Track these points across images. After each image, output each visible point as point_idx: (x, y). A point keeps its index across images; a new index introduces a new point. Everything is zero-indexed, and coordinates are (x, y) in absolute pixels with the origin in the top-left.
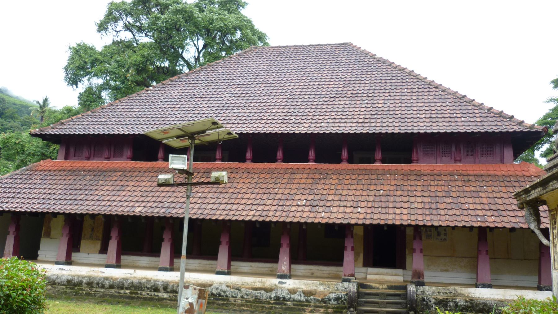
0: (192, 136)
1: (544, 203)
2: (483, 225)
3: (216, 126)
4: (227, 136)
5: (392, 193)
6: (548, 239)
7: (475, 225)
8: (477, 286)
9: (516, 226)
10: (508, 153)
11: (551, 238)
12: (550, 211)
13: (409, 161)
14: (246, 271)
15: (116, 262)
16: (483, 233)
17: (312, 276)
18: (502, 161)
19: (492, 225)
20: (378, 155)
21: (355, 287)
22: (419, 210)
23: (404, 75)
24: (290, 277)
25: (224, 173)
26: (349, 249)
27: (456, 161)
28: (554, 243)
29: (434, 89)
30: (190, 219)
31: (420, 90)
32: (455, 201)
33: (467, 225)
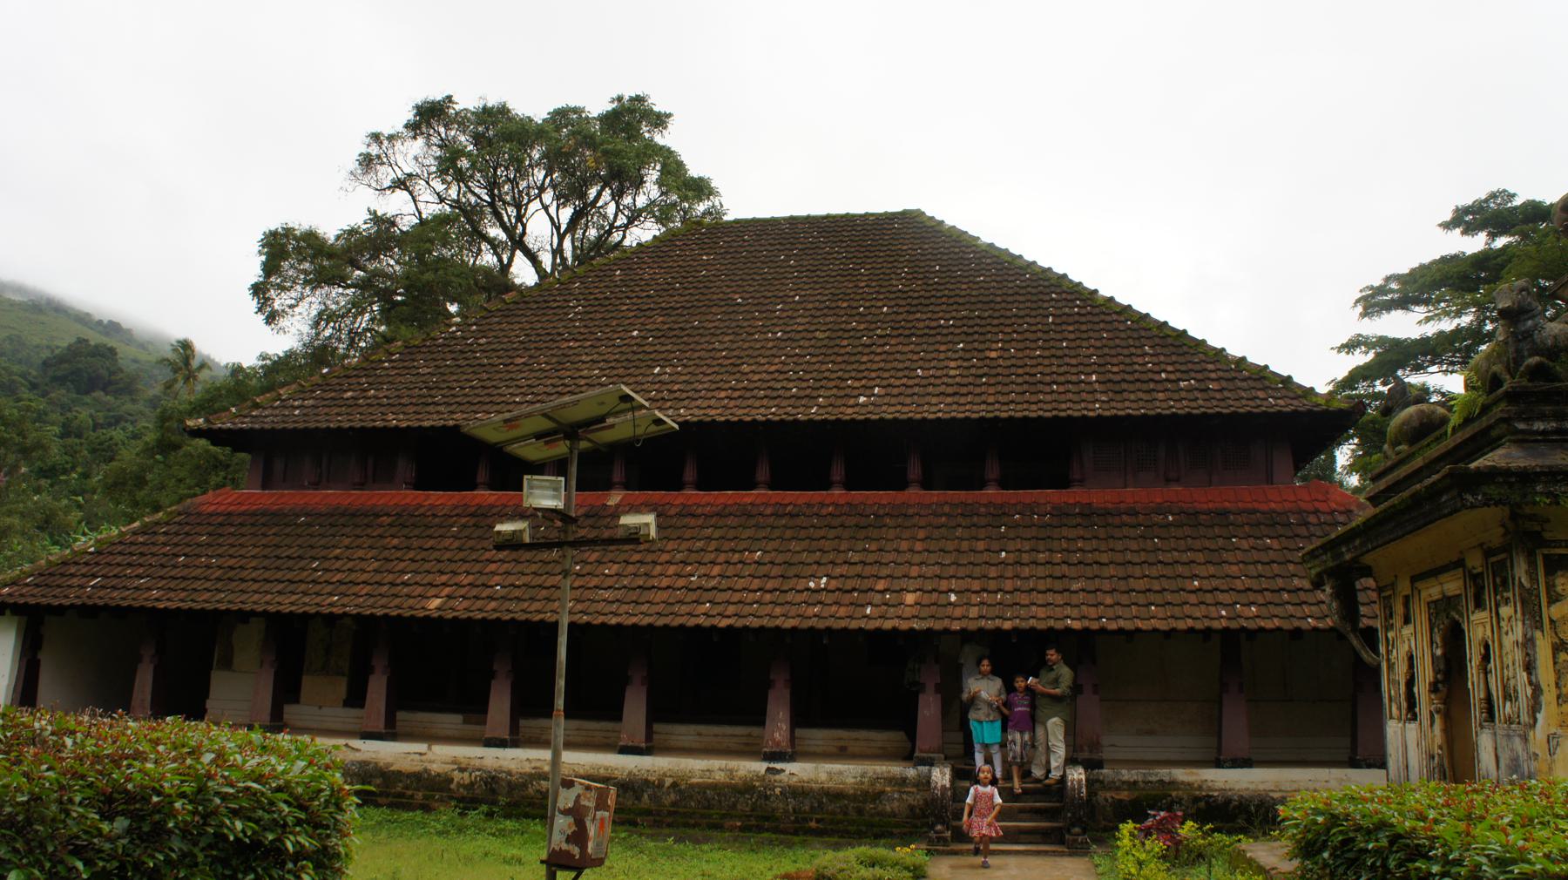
0: (571, 431)
1: (1367, 571)
2: (1234, 625)
3: (628, 405)
4: (653, 428)
5: (1026, 558)
6: (1376, 651)
7: (1216, 625)
8: (1218, 764)
9: (1303, 625)
10: (1283, 461)
11: (1382, 650)
12: (1380, 590)
13: (1063, 483)
14: (686, 745)
15: (386, 726)
16: (1232, 642)
17: (842, 754)
18: (1269, 480)
19: (1251, 625)
20: (993, 471)
21: (948, 777)
24: (791, 758)
25: (650, 519)
26: (930, 688)
27: (1168, 481)
28: (1388, 660)
30: (572, 625)
31: (1083, 319)
32: (1168, 571)
33: (1199, 625)
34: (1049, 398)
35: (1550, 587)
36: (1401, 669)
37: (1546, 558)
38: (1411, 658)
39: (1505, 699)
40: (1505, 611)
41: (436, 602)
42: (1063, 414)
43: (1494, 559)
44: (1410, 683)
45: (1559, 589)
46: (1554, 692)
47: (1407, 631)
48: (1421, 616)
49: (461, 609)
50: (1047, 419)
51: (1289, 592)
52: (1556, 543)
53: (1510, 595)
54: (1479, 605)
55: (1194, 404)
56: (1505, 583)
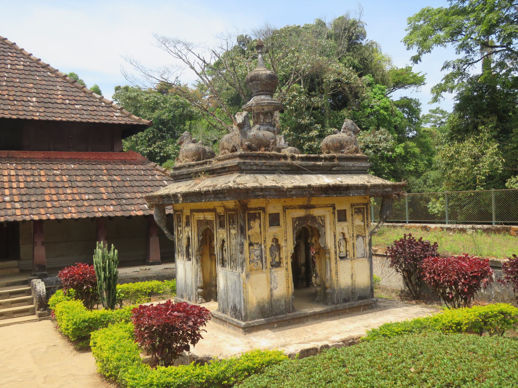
2: (105, 215)
6: (173, 234)
11: (175, 233)
22: (40, 203)
23: (5, 46)
29: (42, 69)
34: (13, 108)
35: (249, 223)
36: (184, 242)
37: (249, 214)
38: (188, 238)
39: (231, 260)
40: (233, 232)
42: (22, 117)
43: (230, 213)
44: (188, 247)
45: (251, 225)
46: (249, 260)
47: (187, 229)
48: (194, 224)
50: (14, 119)
51: (125, 199)
52: (252, 209)
53: (234, 226)
54: (222, 226)
55: (82, 117)
56: (233, 222)
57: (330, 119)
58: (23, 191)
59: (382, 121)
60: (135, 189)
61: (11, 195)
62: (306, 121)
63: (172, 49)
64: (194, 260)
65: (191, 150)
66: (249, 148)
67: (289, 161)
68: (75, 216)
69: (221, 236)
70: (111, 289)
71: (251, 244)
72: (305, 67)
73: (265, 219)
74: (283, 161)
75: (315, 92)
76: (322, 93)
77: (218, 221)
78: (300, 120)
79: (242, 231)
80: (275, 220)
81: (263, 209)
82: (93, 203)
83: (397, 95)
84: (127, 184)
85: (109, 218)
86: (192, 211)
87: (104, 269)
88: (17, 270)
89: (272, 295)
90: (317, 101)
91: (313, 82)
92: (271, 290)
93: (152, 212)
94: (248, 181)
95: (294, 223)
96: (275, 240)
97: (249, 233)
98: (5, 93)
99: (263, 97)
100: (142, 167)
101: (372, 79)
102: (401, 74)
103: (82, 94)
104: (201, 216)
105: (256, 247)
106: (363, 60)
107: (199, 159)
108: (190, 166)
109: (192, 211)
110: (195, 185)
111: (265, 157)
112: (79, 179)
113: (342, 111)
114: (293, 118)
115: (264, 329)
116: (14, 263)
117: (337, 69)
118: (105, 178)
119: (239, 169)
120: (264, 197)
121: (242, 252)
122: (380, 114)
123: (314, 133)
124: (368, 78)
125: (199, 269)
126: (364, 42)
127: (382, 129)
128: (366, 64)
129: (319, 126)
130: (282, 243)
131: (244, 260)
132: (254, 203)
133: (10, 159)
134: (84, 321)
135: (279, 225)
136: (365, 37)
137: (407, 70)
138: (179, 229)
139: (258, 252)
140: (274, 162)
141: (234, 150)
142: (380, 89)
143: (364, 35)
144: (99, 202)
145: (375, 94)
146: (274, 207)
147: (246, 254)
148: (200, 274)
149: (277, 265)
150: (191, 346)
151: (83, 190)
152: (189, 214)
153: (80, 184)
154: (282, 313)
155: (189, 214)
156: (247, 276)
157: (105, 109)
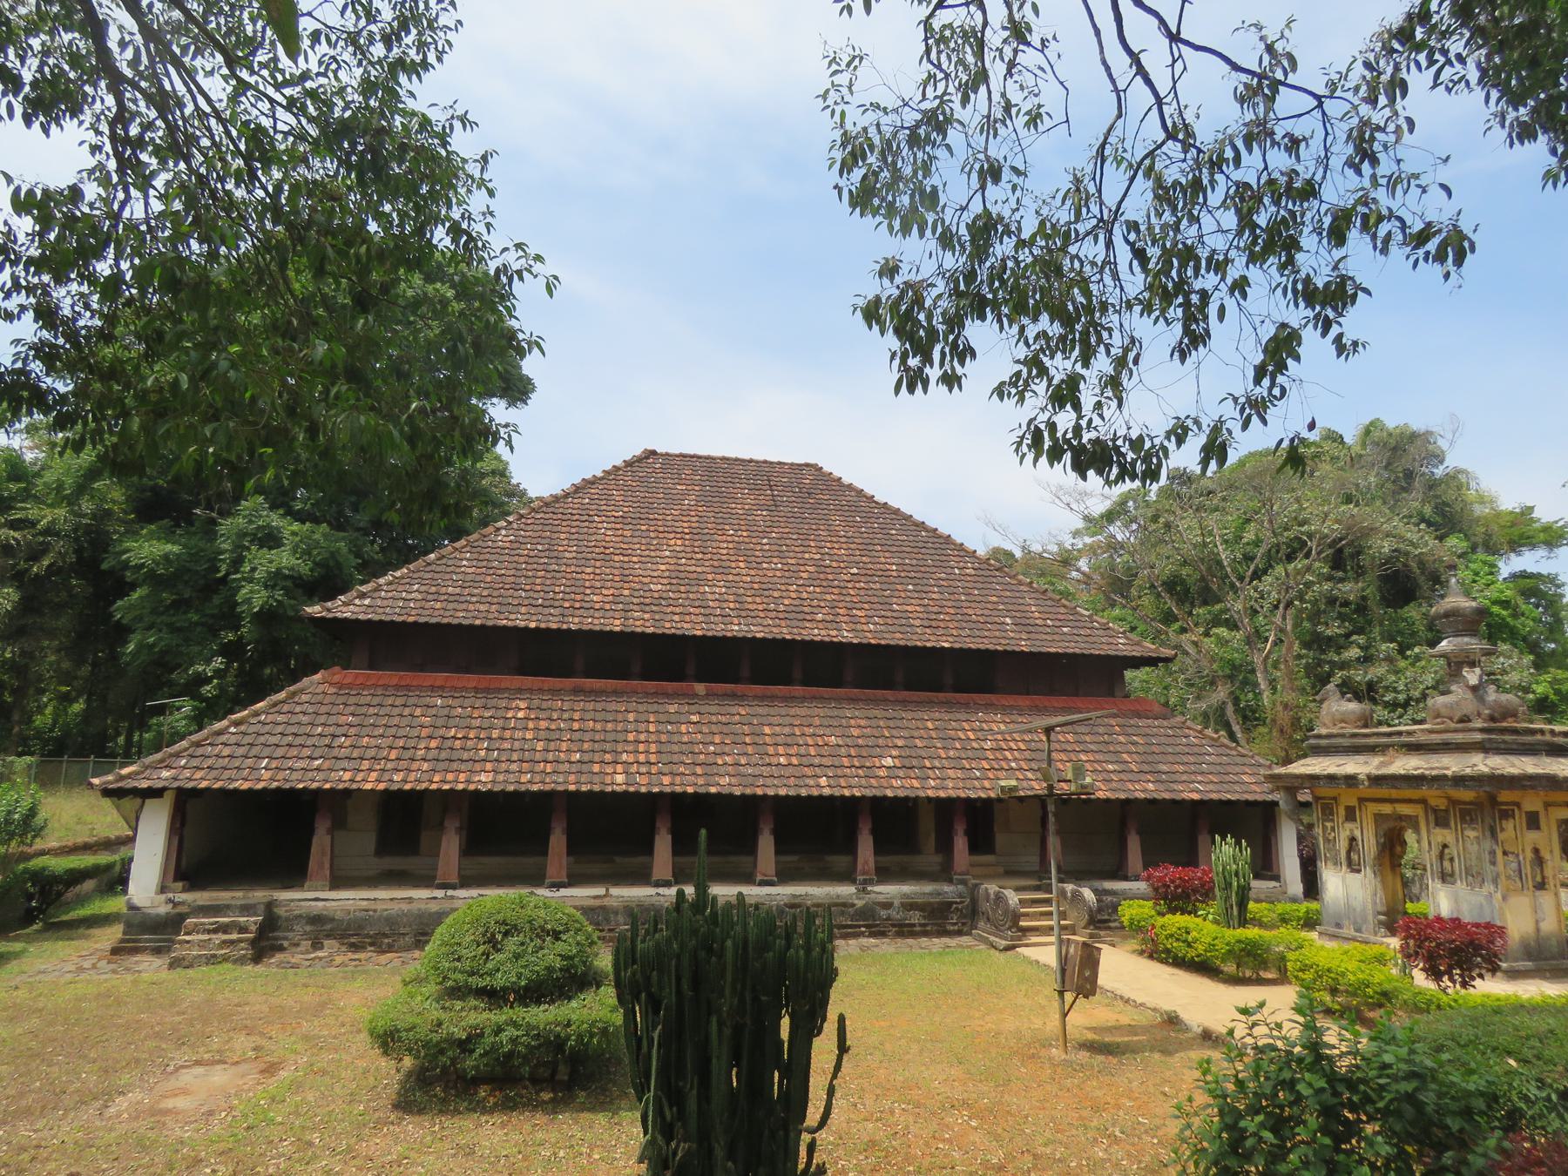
36: (1343, 845)
38: (1353, 839)
41: (620, 778)
47: (1348, 825)
49: (643, 785)
57: (1381, 624)
58: (1027, 754)
59: (1489, 626)
60: (1170, 758)
61: (1015, 759)
62: (1334, 629)
63: (1074, 506)
64: (1368, 872)
65: (1353, 712)
66: (1492, 719)
67: (1548, 737)
68: (1109, 795)
69: (1440, 839)
70: (1242, 905)
71: (1505, 853)
72: (1331, 528)
73: (1520, 819)
74: (1539, 737)
75: (1345, 571)
76: (1359, 575)
77: (1432, 818)
78: (1320, 628)
79: (1494, 835)
80: (1533, 822)
81: (1518, 805)
82: (1122, 776)
83: (1510, 565)
84: (1154, 749)
85: (1153, 801)
86: (1361, 800)
87: (1237, 874)
88: (1001, 870)
89: (1538, 930)
90: (1349, 589)
91: (1343, 557)
92: (1537, 922)
93: (1276, 797)
94: (1482, 764)
95: (1559, 827)
96: (1536, 851)
97: (1501, 836)
98: (970, 611)
99: (1466, 639)
100: (1165, 723)
101: (1465, 544)
102: (1513, 524)
103: (1062, 610)
104: (1387, 809)
105: (1511, 858)
106: (1442, 508)
107: (1366, 726)
108: (1354, 735)
109: (1361, 800)
110: (1383, 764)
111: (1515, 731)
112: (1088, 738)
113: (1406, 609)
114: (1306, 624)
115: (1533, 977)
116: (990, 858)
117: (1395, 532)
118: (1121, 739)
119: (1484, 748)
120: (1533, 787)
121: (1493, 863)
122: (1491, 614)
123: (1354, 652)
124: (1455, 542)
125: (1379, 886)
126: (1439, 472)
127: (1504, 647)
128: (1448, 511)
129: (1361, 639)
130: (1545, 854)
131: (1498, 875)
132: (1505, 796)
133: (988, 707)
134: (1239, 941)
135: (1538, 828)
136: (1441, 462)
137: (1522, 513)
138: (1329, 825)
139: (1514, 866)
140: (1529, 739)
141: (1465, 719)
142: (1485, 563)
143: (1439, 458)
144: (1130, 776)
145: (1476, 574)
146: (1532, 803)
147: (1500, 867)
148: (1380, 893)
149: (1541, 886)
150: (1488, 976)
151: (1099, 757)
152: (1354, 802)
153: (1092, 747)
154: (1553, 958)
155: (1354, 802)
156: (1504, 898)
157: (1101, 632)
